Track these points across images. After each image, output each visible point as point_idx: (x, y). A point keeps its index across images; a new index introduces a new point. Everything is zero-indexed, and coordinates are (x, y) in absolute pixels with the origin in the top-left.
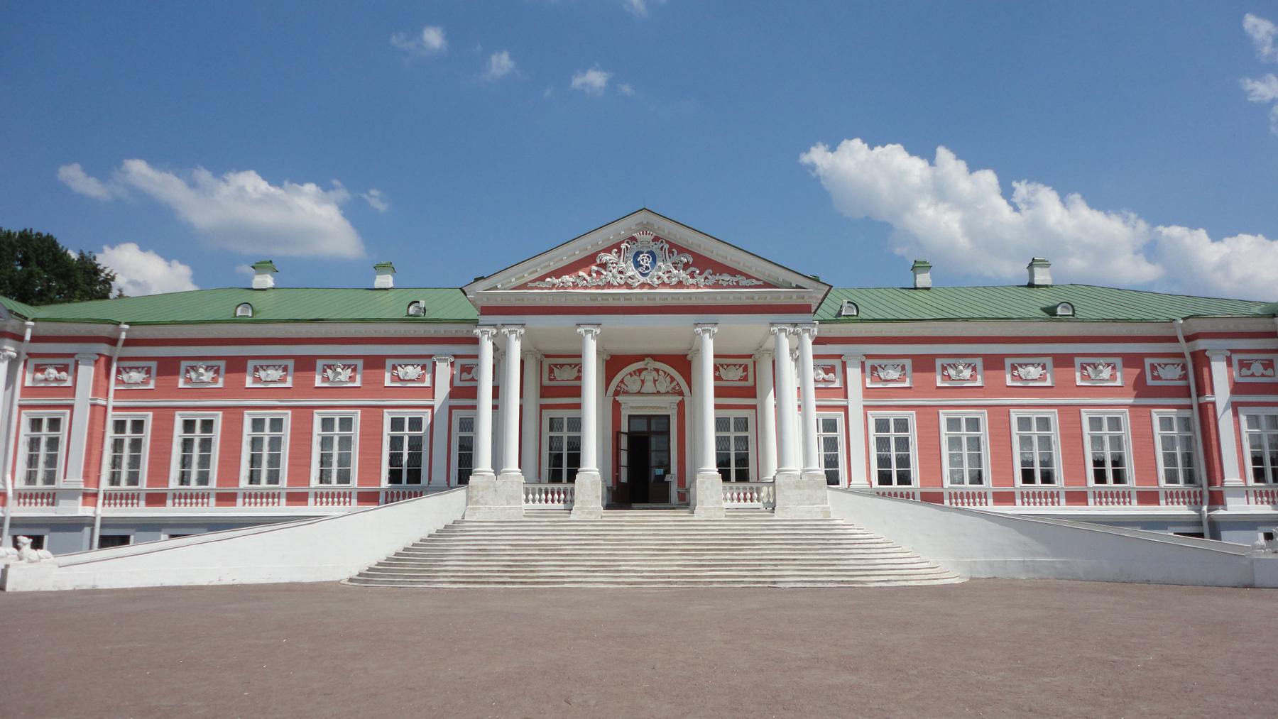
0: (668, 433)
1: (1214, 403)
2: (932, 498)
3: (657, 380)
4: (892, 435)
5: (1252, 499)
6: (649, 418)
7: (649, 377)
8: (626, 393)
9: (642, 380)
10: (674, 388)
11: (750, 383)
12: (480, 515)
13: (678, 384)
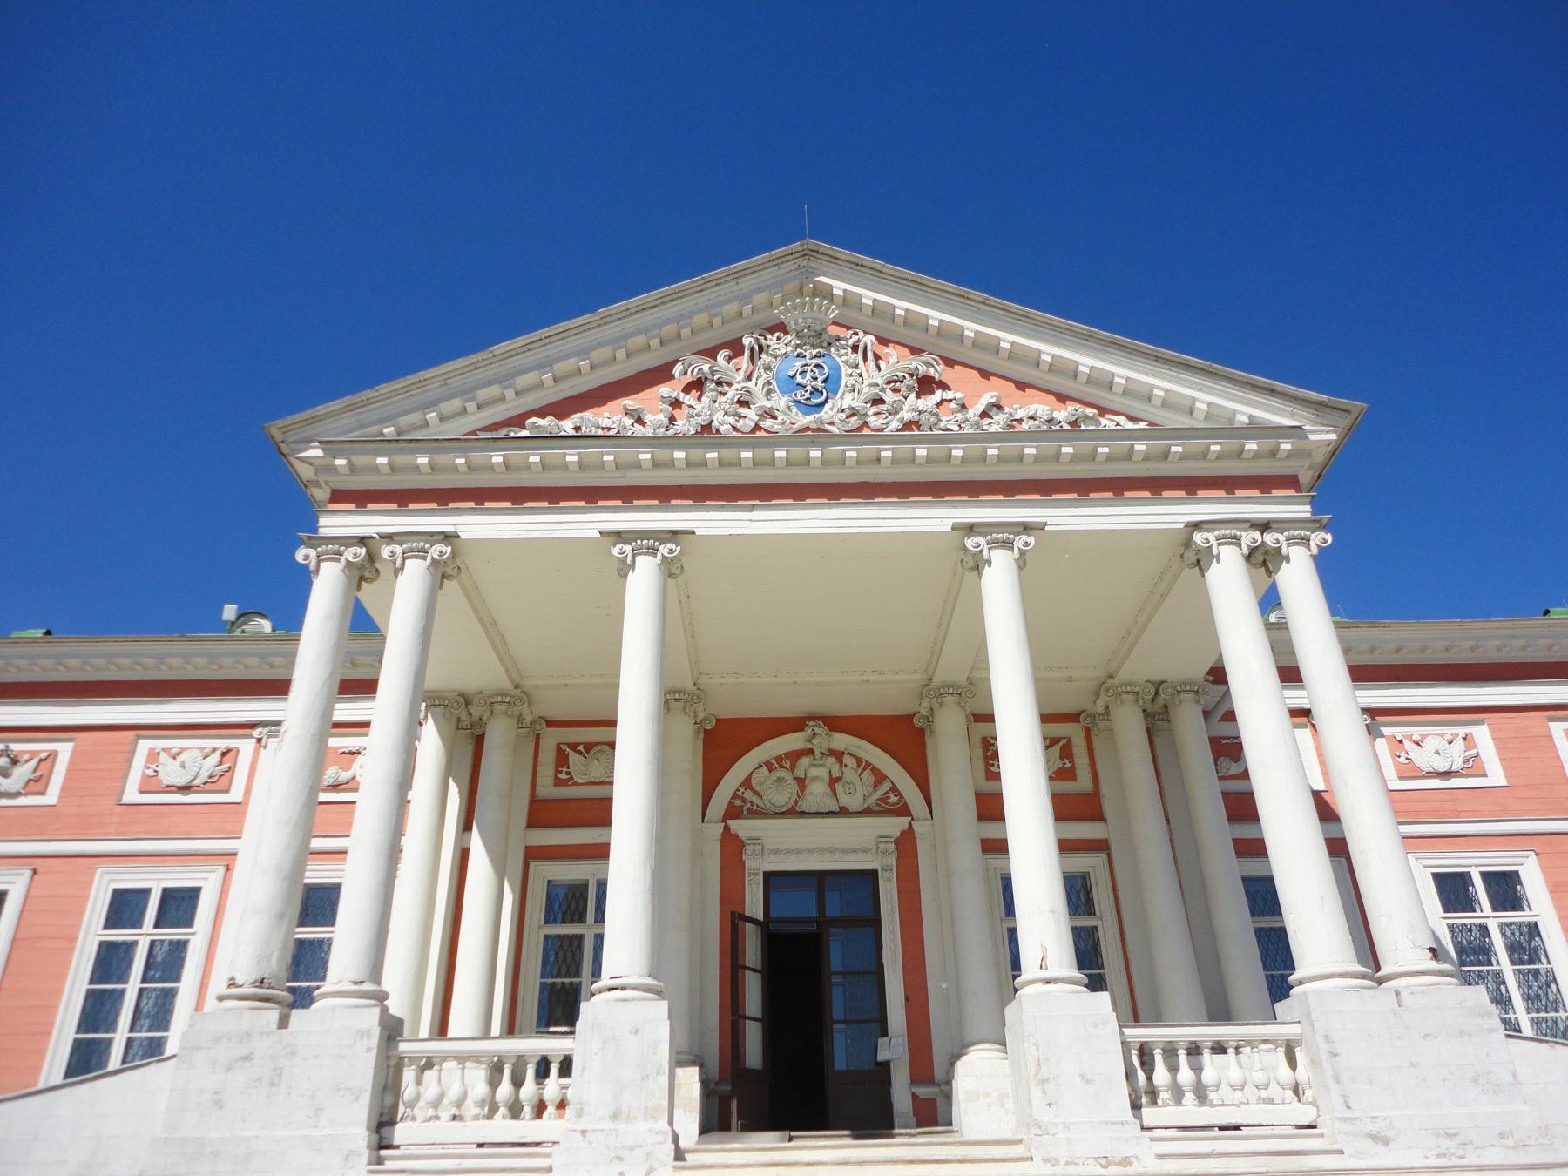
0: (875, 922)
3: (838, 779)
6: (820, 879)
7: (817, 772)
8: (758, 813)
9: (795, 778)
10: (884, 799)
11: (1083, 783)
13: (894, 789)
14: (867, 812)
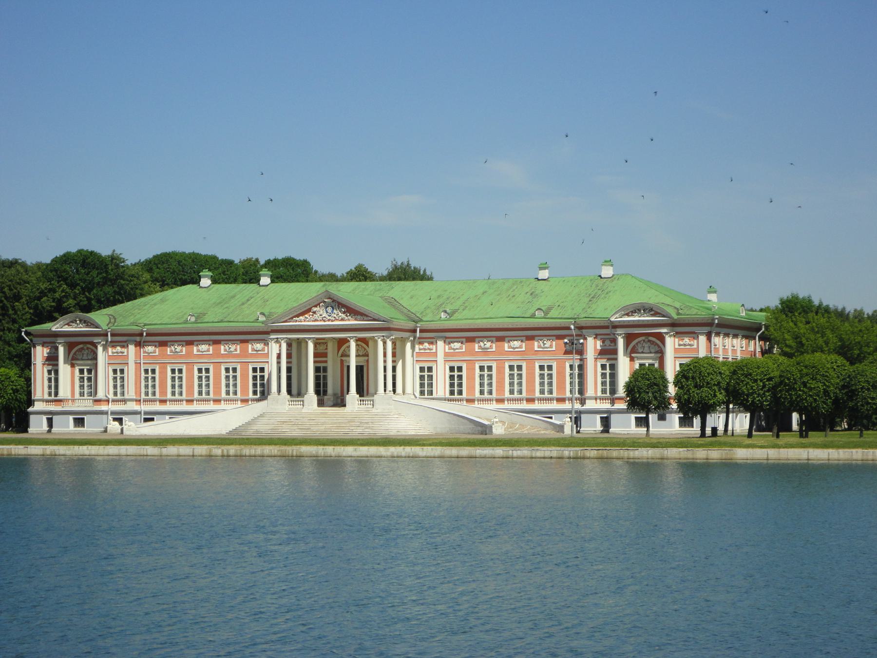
4: (456, 373)
5: (598, 401)
12: (304, 411)
14: (363, 356)
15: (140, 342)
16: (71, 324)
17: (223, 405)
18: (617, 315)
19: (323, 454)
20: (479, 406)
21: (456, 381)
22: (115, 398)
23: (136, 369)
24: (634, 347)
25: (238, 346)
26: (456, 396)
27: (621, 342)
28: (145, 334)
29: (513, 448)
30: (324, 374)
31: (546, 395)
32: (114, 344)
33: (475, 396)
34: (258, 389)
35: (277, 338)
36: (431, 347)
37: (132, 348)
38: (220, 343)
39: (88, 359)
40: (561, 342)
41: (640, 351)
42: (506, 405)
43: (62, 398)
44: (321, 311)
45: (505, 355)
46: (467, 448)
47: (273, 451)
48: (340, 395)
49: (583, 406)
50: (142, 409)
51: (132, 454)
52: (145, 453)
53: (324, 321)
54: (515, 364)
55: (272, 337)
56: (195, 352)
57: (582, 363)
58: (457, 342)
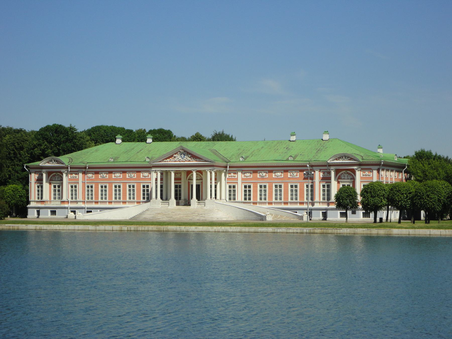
1: (315, 182)
2: (254, 203)
4: (248, 189)
5: (321, 204)
12: (169, 207)
14: (199, 180)
15: (85, 172)
16: (50, 162)
17: (127, 205)
18: (331, 160)
19: (179, 230)
20: (259, 206)
21: (247, 193)
22: (72, 200)
23: (83, 185)
24: (340, 176)
25: (135, 174)
26: (247, 201)
27: (333, 173)
28: (87, 168)
29: (277, 228)
30: (180, 189)
31: (294, 201)
32: (71, 173)
33: (272, 200)
34: (146, 196)
35: (156, 170)
36: (235, 175)
37: (81, 175)
38: (126, 173)
39: (58, 180)
40: (302, 173)
41: (343, 178)
42: (273, 206)
43: (45, 200)
44: (178, 156)
45: (273, 180)
46: (254, 227)
47: (153, 228)
48: (187, 200)
49: (313, 206)
50: (86, 206)
51: (81, 229)
52: (88, 229)
53: (180, 162)
54: (278, 184)
55: (153, 169)
56: (113, 177)
57: (312, 184)
58: (248, 173)
